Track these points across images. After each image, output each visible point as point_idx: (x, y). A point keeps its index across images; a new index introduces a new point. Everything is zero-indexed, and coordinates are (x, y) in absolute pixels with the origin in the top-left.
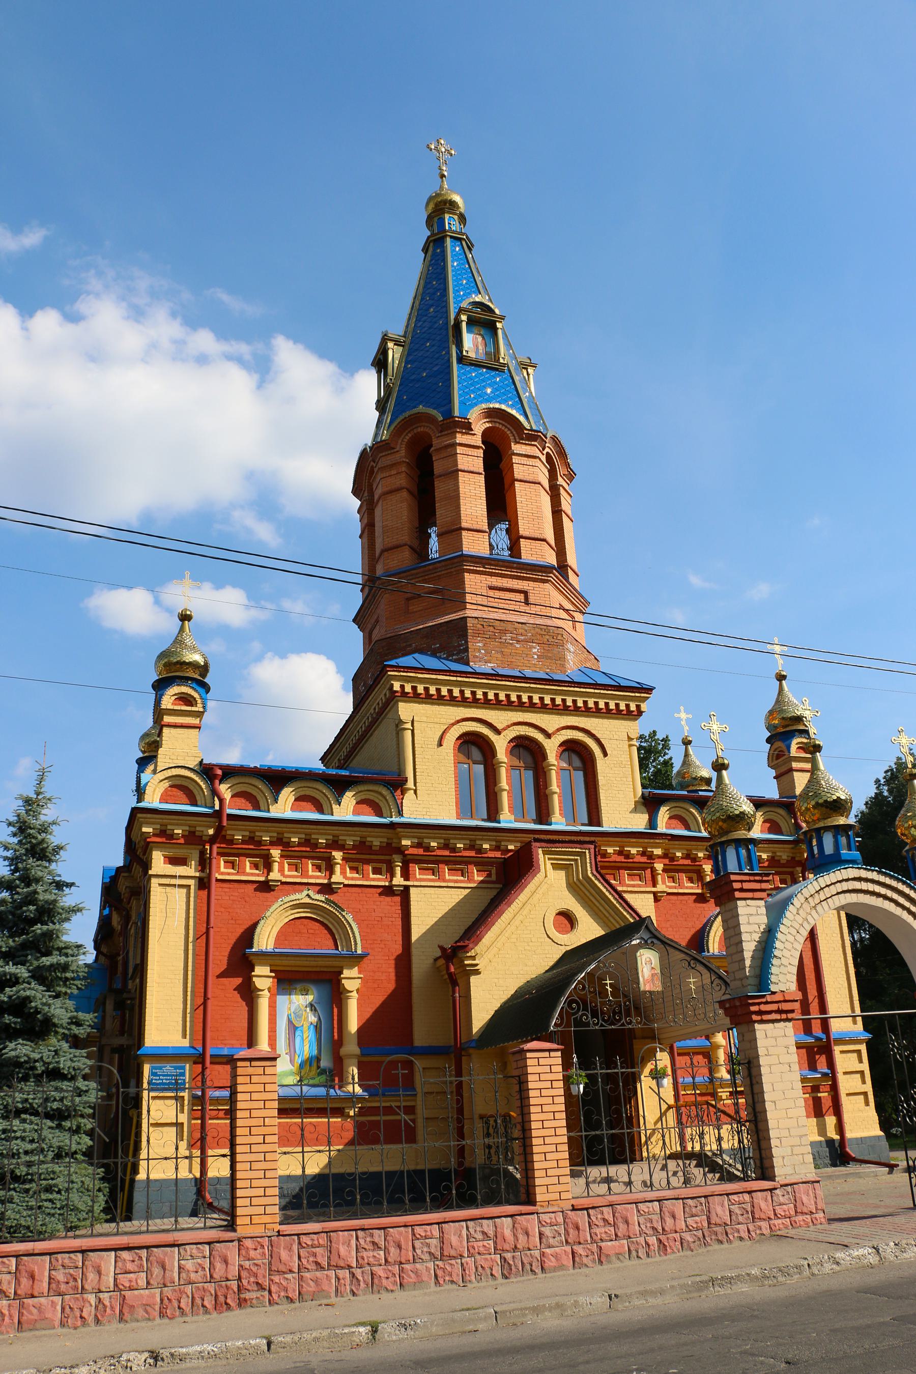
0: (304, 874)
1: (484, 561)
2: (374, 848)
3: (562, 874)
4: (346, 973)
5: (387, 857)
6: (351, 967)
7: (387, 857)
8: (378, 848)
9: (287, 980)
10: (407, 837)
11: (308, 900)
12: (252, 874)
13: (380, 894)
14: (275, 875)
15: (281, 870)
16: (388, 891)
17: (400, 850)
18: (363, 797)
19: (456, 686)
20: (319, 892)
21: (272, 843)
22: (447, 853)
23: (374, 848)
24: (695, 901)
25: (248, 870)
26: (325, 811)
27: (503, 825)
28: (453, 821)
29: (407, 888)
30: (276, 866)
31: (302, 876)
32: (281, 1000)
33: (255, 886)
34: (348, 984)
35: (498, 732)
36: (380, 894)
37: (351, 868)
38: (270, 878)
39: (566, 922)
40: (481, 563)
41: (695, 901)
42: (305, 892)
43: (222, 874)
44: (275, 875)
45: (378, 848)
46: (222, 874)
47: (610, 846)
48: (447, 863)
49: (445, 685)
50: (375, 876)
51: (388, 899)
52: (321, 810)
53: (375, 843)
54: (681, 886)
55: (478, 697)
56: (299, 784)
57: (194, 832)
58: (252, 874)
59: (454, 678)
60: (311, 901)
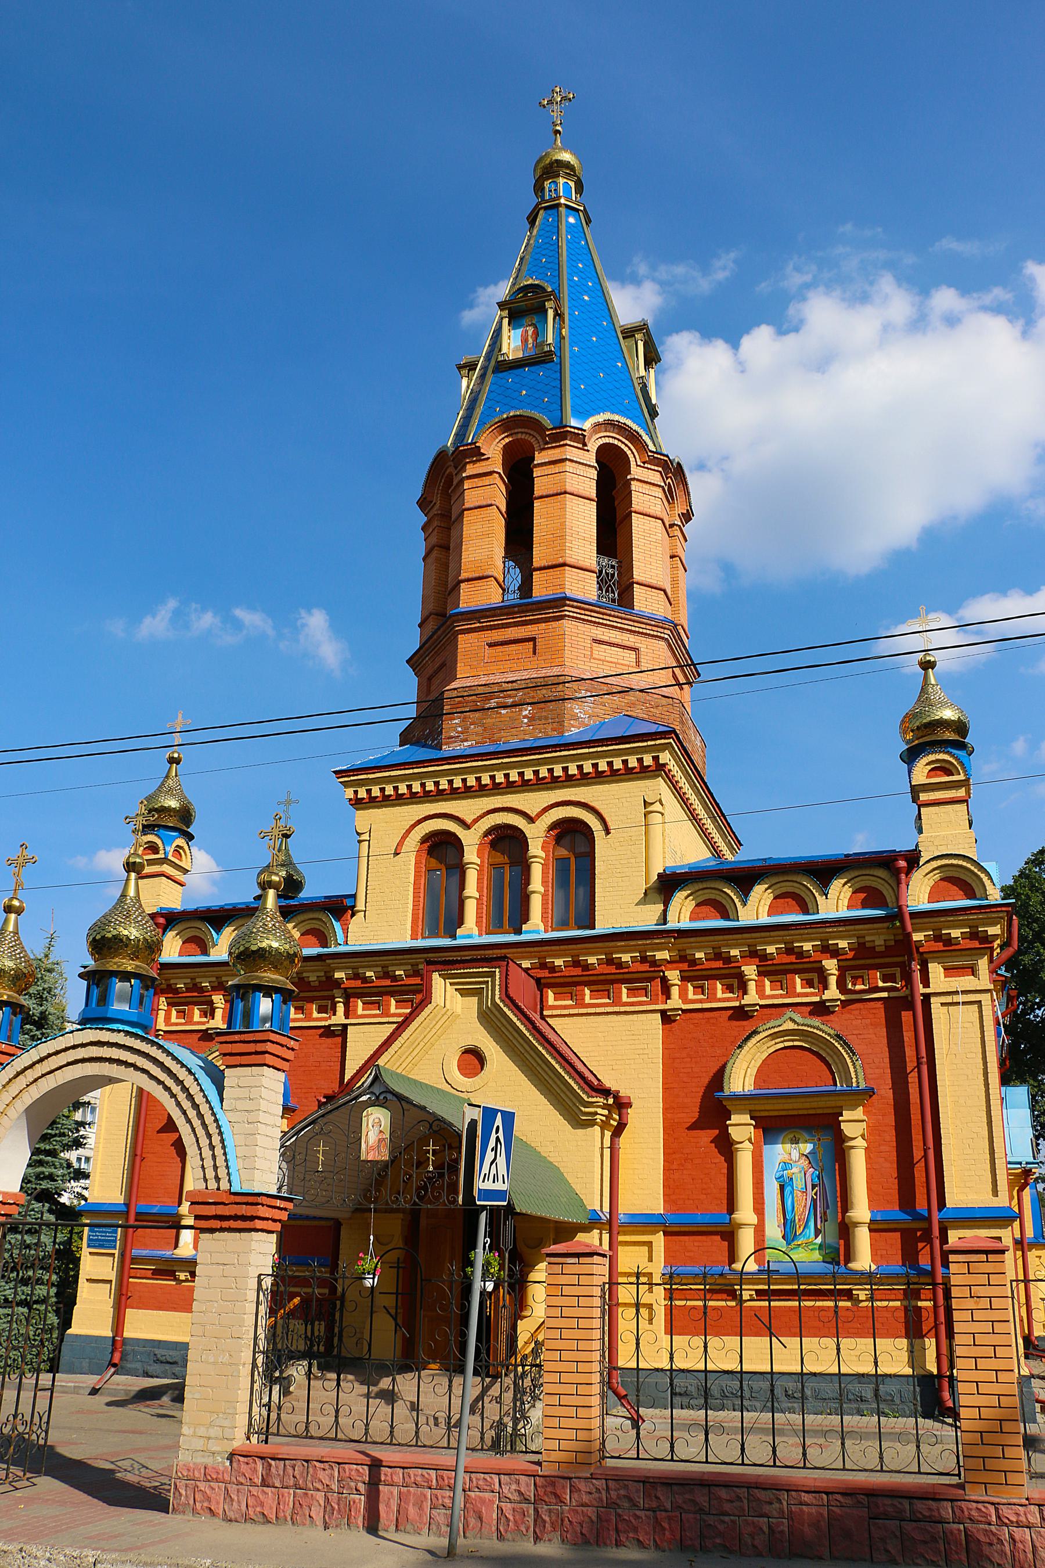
0: (791, 992)
1: (477, 615)
2: (877, 949)
3: (474, 1000)
4: (847, 1115)
5: (329, 993)
6: (853, 1108)
7: (329, 993)
8: (883, 949)
9: (772, 1126)
10: (340, 969)
11: (790, 1026)
12: (806, 995)
13: (321, 1036)
14: (752, 997)
15: (683, 995)
16: (327, 1032)
17: (338, 983)
18: (308, 927)
19: (415, 780)
20: (812, 1014)
21: (215, 989)
22: (388, 982)
23: (877, 949)
24: (730, 1018)
25: (799, 989)
26: (811, 911)
27: (822, 915)
28: (409, 943)
29: (345, 1027)
30: (752, 986)
31: (614, 1004)
32: (766, 1148)
33: (809, 1009)
34: (847, 1129)
35: (467, 826)
36: (321, 1036)
37: (296, 1008)
38: (824, 997)
39: (476, 1062)
40: (476, 618)
41: (730, 1018)
42: (786, 1017)
43: (295, 1020)
44: (752, 997)
45: (883, 949)
46: (295, 1020)
47: (558, 957)
48: (392, 994)
49: (402, 781)
50: (320, 1015)
51: (329, 1041)
52: (725, 916)
53: (877, 943)
54: (309, 1018)
55: (497, 781)
56: (181, 926)
57: (864, 943)
58: (806, 995)
59: (411, 771)
60: (796, 1027)
